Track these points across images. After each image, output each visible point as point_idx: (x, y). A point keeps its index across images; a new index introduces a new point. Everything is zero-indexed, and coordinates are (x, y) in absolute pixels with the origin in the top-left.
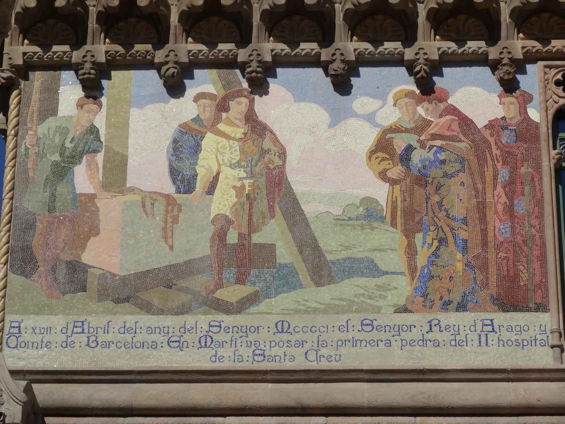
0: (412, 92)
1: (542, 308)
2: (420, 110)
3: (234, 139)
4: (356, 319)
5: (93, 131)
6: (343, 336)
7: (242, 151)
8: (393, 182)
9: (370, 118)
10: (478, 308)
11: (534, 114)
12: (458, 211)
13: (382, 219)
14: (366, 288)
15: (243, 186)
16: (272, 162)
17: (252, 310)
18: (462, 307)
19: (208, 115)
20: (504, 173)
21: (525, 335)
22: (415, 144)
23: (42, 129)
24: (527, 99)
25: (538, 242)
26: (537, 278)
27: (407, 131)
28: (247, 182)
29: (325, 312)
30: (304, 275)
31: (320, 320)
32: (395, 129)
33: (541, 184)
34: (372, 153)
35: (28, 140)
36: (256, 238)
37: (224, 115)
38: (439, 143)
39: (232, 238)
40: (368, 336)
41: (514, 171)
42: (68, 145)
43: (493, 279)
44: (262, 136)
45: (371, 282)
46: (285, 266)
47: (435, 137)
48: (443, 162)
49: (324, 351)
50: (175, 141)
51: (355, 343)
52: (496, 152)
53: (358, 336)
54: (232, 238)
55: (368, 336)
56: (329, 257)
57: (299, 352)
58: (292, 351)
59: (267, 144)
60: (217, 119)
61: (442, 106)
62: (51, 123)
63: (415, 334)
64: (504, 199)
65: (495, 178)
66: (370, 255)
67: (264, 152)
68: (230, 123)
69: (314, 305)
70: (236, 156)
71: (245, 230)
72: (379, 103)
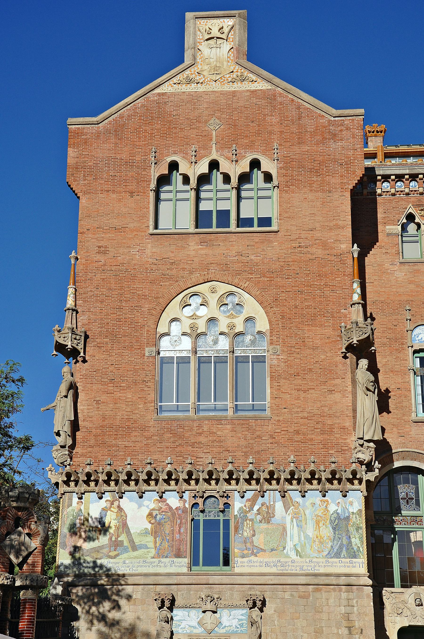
0: (158, 499)
1: (185, 557)
2: (160, 504)
3: (114, 512)
4: (142, 560)
5: (81, 510)
6: (139, 565)
7: (116, 515)
8: (152, 524)
9: (147, 507)
10: (170, 557)
11: (187, 506)
12: (167, 532)
13: (149, 534)
14: (144, 552)
15: (117, 525)
16: (123, 518)
17: (117, 558)
18: (167, 557)
19: (109, 505)
20: (179, 521)
21: (181, 564)
22: (158, 514)
23: (68, 510)
24: (185, 501)
25: (186, 540)
26: (185, 550)
27: (156, 510)
28: (117, 524)
29: (135, 558)
30: (130, 549)
31: (134, 560)
32: (153, 509)
33: (187, 525)
34: (148, 516)
35: (65, 513)
36: (119, 539)
37: (112, 506)
38: (164, 513)
39: (113, 539)
40: (144, 565)
41: (181, 521)
42: (75, 514)
43: (174, 550)
44: (121, 511)
45: (146, 550)
46: (126, 546)
47: (163, 512)
48: (164, 518)
49: (134, 568)
50: (100, 513)
51: (141, 566)
52: (177, 516)
53: (142, 565)
54: (113, 539)
55: (144, 565)
56: (136, 544)
57: (128, 569)
58: (126, 568)
59: (123, 514)
60: (111, 507)
61: (165, 503)
62: (70, 508)
63: (155, 564)
64: (178, 528)
65: (177, 523)
66: (146, 543)
67: (122, 516)
68: (114, 508)
69: (132, 556)
70: (115, 517)
71: (116, 537)
72: (150, 502)
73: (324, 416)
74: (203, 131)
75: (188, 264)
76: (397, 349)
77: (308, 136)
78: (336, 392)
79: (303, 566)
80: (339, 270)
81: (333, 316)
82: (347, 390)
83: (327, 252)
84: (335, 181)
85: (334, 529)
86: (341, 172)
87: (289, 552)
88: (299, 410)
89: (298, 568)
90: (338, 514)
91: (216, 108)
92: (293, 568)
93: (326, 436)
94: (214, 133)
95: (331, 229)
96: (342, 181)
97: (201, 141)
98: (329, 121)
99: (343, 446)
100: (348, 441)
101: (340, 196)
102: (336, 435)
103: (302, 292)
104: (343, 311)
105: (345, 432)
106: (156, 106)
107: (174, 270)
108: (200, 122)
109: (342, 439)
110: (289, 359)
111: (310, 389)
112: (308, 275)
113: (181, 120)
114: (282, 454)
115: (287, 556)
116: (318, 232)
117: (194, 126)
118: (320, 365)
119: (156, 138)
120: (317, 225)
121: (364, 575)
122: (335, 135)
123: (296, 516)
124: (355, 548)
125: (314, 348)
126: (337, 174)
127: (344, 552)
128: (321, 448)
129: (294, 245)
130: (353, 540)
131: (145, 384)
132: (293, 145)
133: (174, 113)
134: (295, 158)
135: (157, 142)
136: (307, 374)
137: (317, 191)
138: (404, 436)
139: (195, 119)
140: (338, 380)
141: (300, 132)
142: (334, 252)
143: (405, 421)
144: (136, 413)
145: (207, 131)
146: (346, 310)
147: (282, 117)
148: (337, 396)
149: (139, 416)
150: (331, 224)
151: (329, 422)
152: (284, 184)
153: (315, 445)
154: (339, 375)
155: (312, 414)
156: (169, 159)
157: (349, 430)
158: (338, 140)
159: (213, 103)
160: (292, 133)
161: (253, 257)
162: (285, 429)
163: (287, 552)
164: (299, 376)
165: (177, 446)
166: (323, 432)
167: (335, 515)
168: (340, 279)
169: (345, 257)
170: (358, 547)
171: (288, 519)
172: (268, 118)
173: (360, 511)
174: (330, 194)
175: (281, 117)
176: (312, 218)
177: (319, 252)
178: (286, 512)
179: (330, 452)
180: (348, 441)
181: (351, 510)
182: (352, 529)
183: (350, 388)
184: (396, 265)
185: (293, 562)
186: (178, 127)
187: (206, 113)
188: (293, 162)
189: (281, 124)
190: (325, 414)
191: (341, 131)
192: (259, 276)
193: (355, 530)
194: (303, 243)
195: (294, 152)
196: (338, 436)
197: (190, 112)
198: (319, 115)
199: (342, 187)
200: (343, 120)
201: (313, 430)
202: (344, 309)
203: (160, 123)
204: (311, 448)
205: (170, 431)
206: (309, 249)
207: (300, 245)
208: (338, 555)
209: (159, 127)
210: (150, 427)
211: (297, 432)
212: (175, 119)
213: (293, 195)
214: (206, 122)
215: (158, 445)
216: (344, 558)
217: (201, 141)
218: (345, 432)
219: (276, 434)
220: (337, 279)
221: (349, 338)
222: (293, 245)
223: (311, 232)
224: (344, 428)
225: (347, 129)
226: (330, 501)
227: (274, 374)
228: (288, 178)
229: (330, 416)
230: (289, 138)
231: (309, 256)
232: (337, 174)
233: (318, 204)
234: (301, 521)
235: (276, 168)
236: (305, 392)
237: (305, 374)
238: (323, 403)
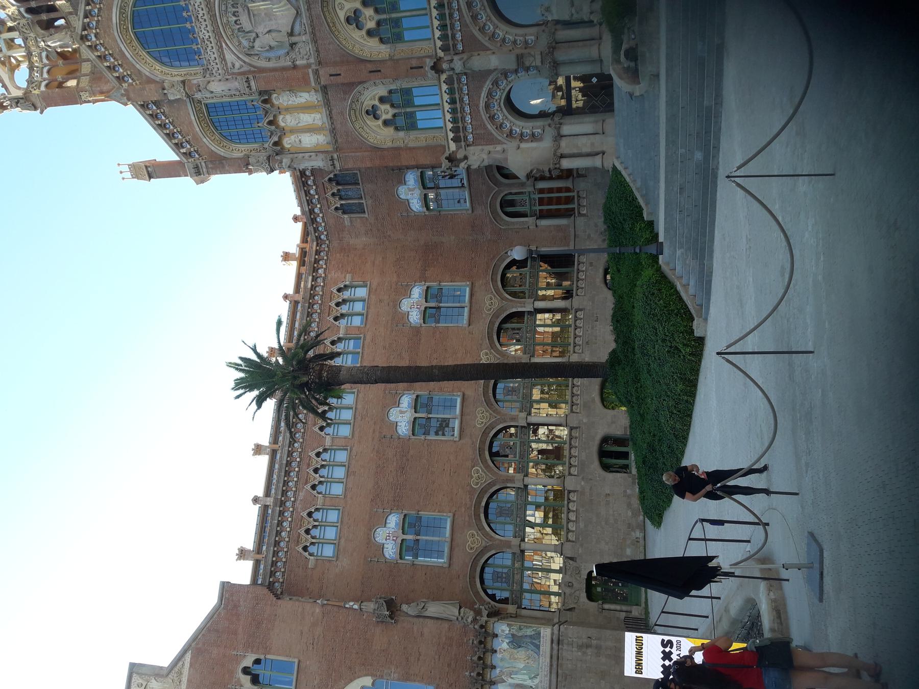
79: (545, 675)
83: (320, 624)
85: (520, 647)
87: (534, 684)
89: (546, 678)
90: (509, 642)
92: (545, 683)
98: (224, 608)
100: (458, 626)
102: (454, 636)
104: (364, 617)
110: (395, 664)
114: (464, 679)
115: (537, 686)
121: (553, 630)
123: (510, 675)
124: (533, 633)
127: (536, 642)
129: (311, 648)
130: (528, 633)
151: (444, 639)
161: (316, 683)
162: (446, 674)
163: (534, 685)
167: (510, 644)
170: (533, 630)
171: (510, 681)
173: (508, 625)
178: (505, 682)
179: (465, 641)
180: (458, 626)
181: (507, 632)
182: (520, 634)
183: (421, 620)
185: (541, 682)
192: (330, 679)
193: (522, 631)
198: (218, 615)
208: (538, 647)
211: (449, 665)
216: (540, 642)
219: (449, 682)
225: (232, 596)
226: (500, 647)
227: (405, 678)
234: (513, 671)
236: (420, 655)
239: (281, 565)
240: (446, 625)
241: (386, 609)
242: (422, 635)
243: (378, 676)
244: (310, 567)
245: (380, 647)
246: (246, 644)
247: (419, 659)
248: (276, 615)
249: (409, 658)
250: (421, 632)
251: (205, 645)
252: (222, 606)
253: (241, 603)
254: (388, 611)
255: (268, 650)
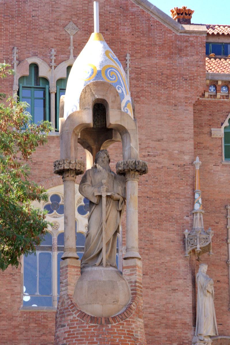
73: (168, 312)
74: (61, 35)
75: (49, 165)
76: (218, 245)
77: (157, 49)
78: (179, 291)
80: (182, 179)
81: (177, 222)
82: (188, 290)
84: (181, 94)
86: (185, 87)
88: (147, 306)
91: (73, 13)
93: (169, 330)
94: (72, 37)
95: (176, 141)
96: (186, 96)
97: (59, 45)
98: (176, 35)
99: (185, 340)
101: (185, 110)
103: (150, 198)
104: (185, 218)
105: (186, 327)
106: (16, 4)
107: (37, 171)
108: (57, 25)
109: (183, 333)
111: (158, 287)
112: (155, 183)
113: (41, 21)
116: (165, 142)
117: (52, 29)
118: (166, 266)
119: (16, 37)
120: (165, 136)
122: (180, 50)
125: (161, 251)
126: (182, 88)
128: (166, 341)
131: (12, 277)
132: (143, 57)
133: (34, 13)
134: (145, 70)
135: (18, 42)
136: (154, 273)
137: (164, 104)
138: (222, 324)
139: (54, 22)
140: (181, 280)
141: (149, 44)
142: (180, 163)
143: (223, 311)
144: (4, 304)
145: (64, 35)
146: (188, 217)
147: (133, 27)
148: (179, 295)
149: (7, 307)
150: (176, 136)
151: (173, 318)
152: (135, 95)
153: (161, 337)
154: (182, 276)
155: (158, 310)
156: (31, 61)
157: (189, 326)
158: (184, 56)
159: (70, 7)
160: (143, 45)
164: (147, 275)
165: (41, 335)
166: (167, 326)
168: (183, 188)
169: (188, 168)
172: (121, 27)
174: (175, 108)
175: (133, 27)
176: (160, 129)
177: (166, 162)
183: (190, 289)
184: (219, 166)
186: (37, 28)
187: (64, 16)
188: (144, 73)
189: (133, 35)
190: (169, 311)
191: (186, 47)
194: (152, 152)
195: (144, 63)
196: (180, 330)
197: (48, 14)
198: (167, 29)
199: (187, 101)
200: (188, 36)
201: (159, 325)
202: (187, 216)
203: (20, 23)
204: (157, 340)
205: (36, 321)
206: (156, 158)
207: (149, 154)
209: (19, 26)
210: (17, 317)
212: (34, 19)
213: (143, 105)
214: (64, 26)
215: (25, 333)
217: (59, 45)
218: (186, 327)
220: (181, 188)
221: (193, 244)
222: (143, 153)
223: (158, 142)
224: (185, 324)
225: (191, 46)
228: (139, 89)
229: (173, 312)
230: (140, 50)
231: (157, 165)
232: (182, 88)
233: (165, 115)
235: (129, 78)
236: (153, 289)
237: (153, 274)
238: (168, 300)
239: (212, 92)
240: (189, 319)
241: (203, 246)
242: (174, 290)
243: (124, 239)
244: (212, 129)
245: (155, 240)
246: (139, 69)
247: (147, 288)
248: (175, 106)
249: (148, 276)
250: (177, 289)
251: (132, 15)
252: (178, 34)
253: (184, 59)
254: (200, 248)
255: (136, 99)
